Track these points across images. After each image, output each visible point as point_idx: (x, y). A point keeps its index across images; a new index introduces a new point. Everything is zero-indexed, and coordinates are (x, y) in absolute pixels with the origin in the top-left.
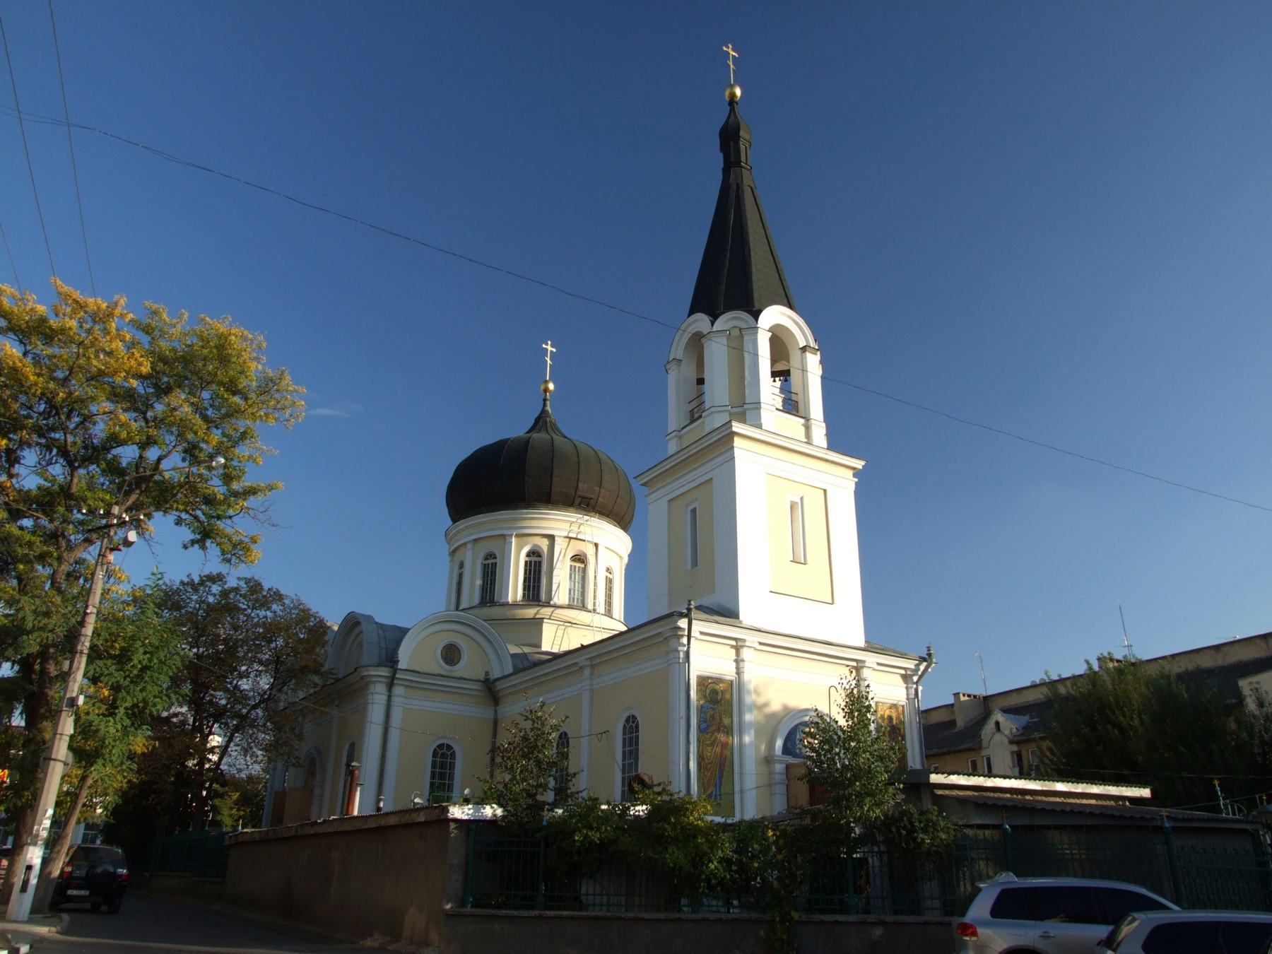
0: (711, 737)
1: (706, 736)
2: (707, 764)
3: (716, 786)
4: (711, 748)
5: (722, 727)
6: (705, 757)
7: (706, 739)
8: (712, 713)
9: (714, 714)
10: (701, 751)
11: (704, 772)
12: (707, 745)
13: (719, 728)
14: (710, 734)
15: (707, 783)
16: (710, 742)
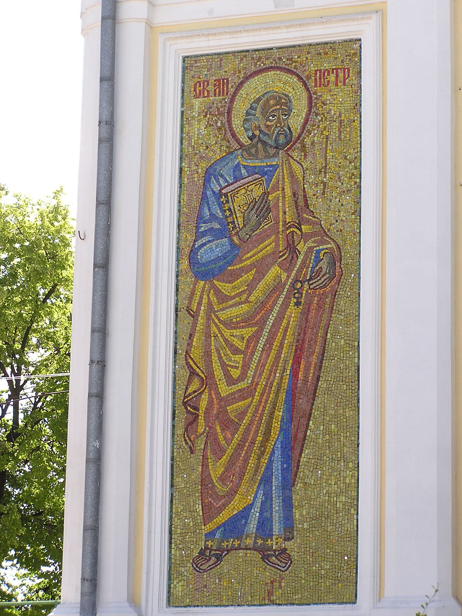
0: (251, 287)
1: (226, 288)
2: (232, 399)
3: (266, 480)
4: (248, 332)
5: (305, 237)
6: (218, 373)
7: (223, 298)
8: (257, 192)
9: (266, 194)
10: (197, 353)
11: (211, 435)
12: (229, 324)
13: (292, 249)
14: (249, 276)
15: (222, 479)
16: (245, 307)
